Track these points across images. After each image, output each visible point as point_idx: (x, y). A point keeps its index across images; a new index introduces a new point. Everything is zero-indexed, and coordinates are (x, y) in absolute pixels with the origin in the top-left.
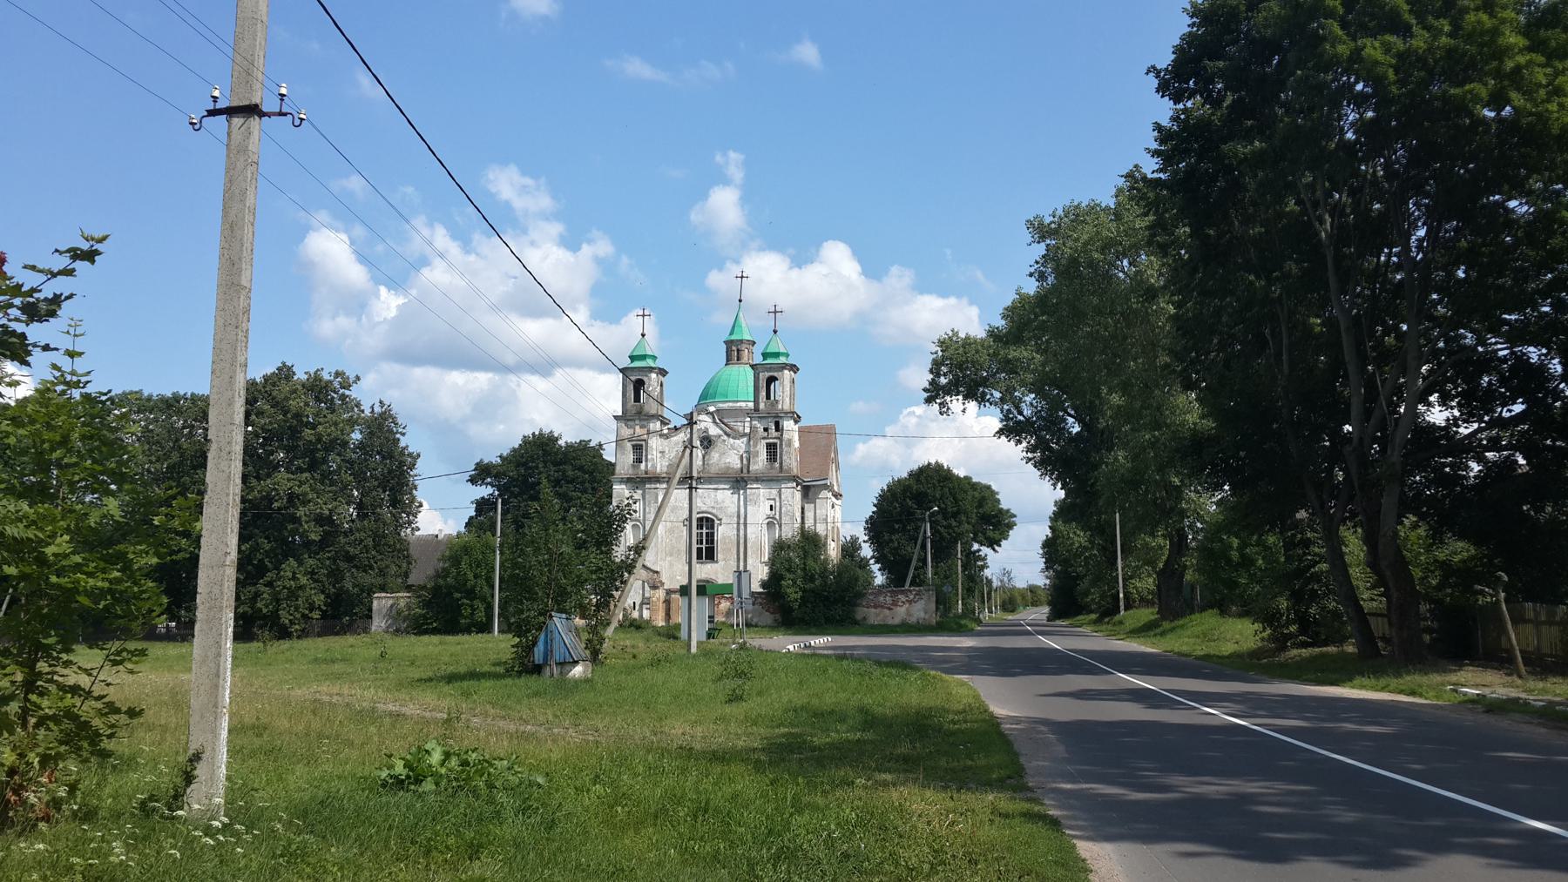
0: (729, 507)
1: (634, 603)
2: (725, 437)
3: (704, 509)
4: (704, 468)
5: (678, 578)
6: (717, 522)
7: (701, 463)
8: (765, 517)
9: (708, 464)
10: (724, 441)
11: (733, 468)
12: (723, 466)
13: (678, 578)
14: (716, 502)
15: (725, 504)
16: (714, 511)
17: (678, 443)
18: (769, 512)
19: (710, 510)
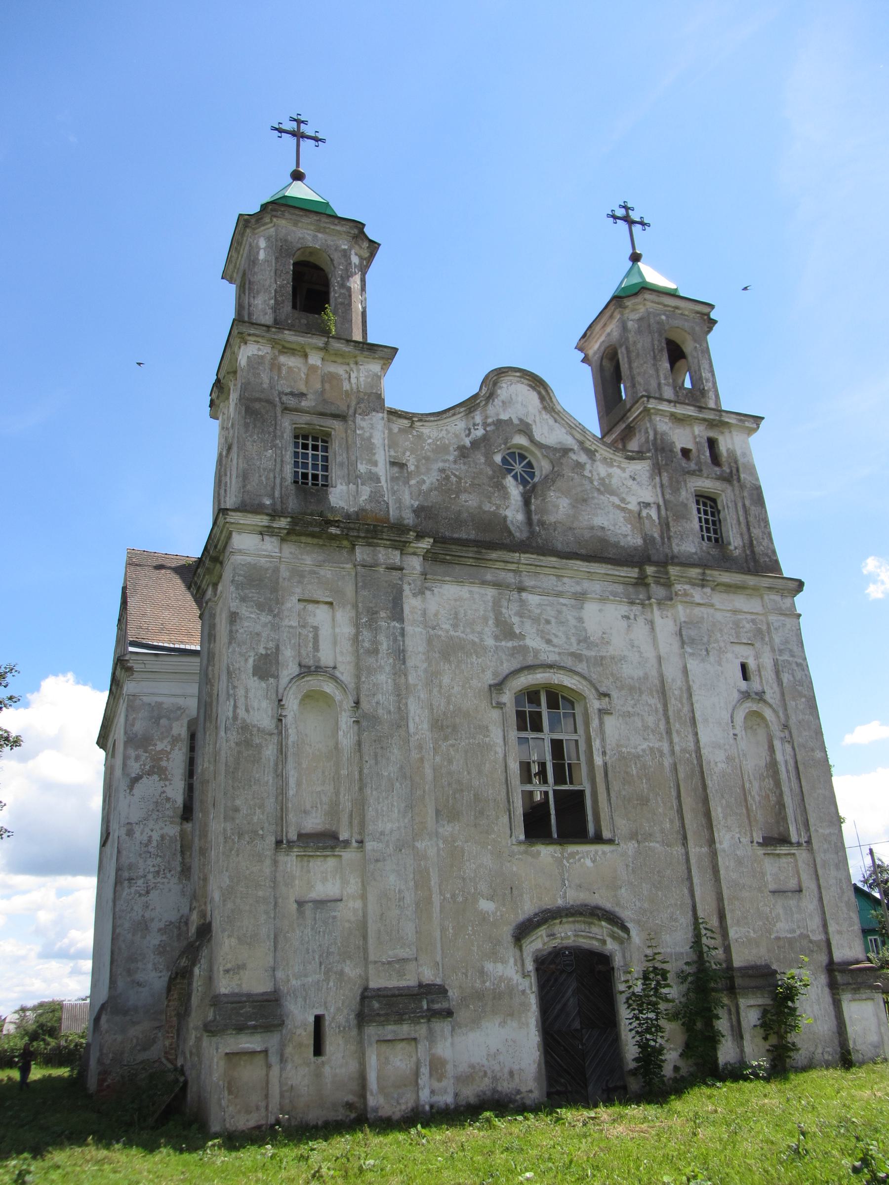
0: (623, 658)
1: (319, 1020)
2: (583, 458)
3: (549, 655)
4: (532, 533)
5: (485, 905)
6: (595, 704)
7: (520, 517)
8: (736, 695)
9: (542, 523)
10: (580, 466)
11: (616, 545)
12: (587, 535)
13: (485, 905)
14: (584, 640)
15: (611, 651)
16: (581, 667)
17: (444, 449)
18: (743, 685)
19: (569, 662)
